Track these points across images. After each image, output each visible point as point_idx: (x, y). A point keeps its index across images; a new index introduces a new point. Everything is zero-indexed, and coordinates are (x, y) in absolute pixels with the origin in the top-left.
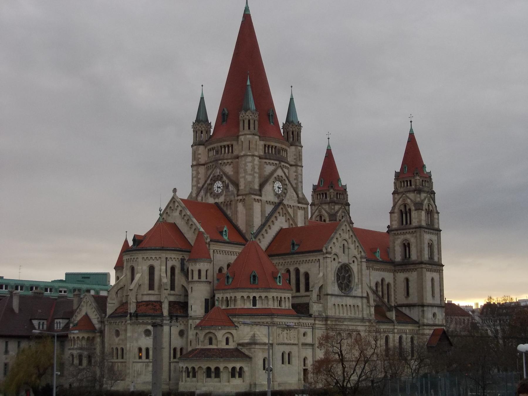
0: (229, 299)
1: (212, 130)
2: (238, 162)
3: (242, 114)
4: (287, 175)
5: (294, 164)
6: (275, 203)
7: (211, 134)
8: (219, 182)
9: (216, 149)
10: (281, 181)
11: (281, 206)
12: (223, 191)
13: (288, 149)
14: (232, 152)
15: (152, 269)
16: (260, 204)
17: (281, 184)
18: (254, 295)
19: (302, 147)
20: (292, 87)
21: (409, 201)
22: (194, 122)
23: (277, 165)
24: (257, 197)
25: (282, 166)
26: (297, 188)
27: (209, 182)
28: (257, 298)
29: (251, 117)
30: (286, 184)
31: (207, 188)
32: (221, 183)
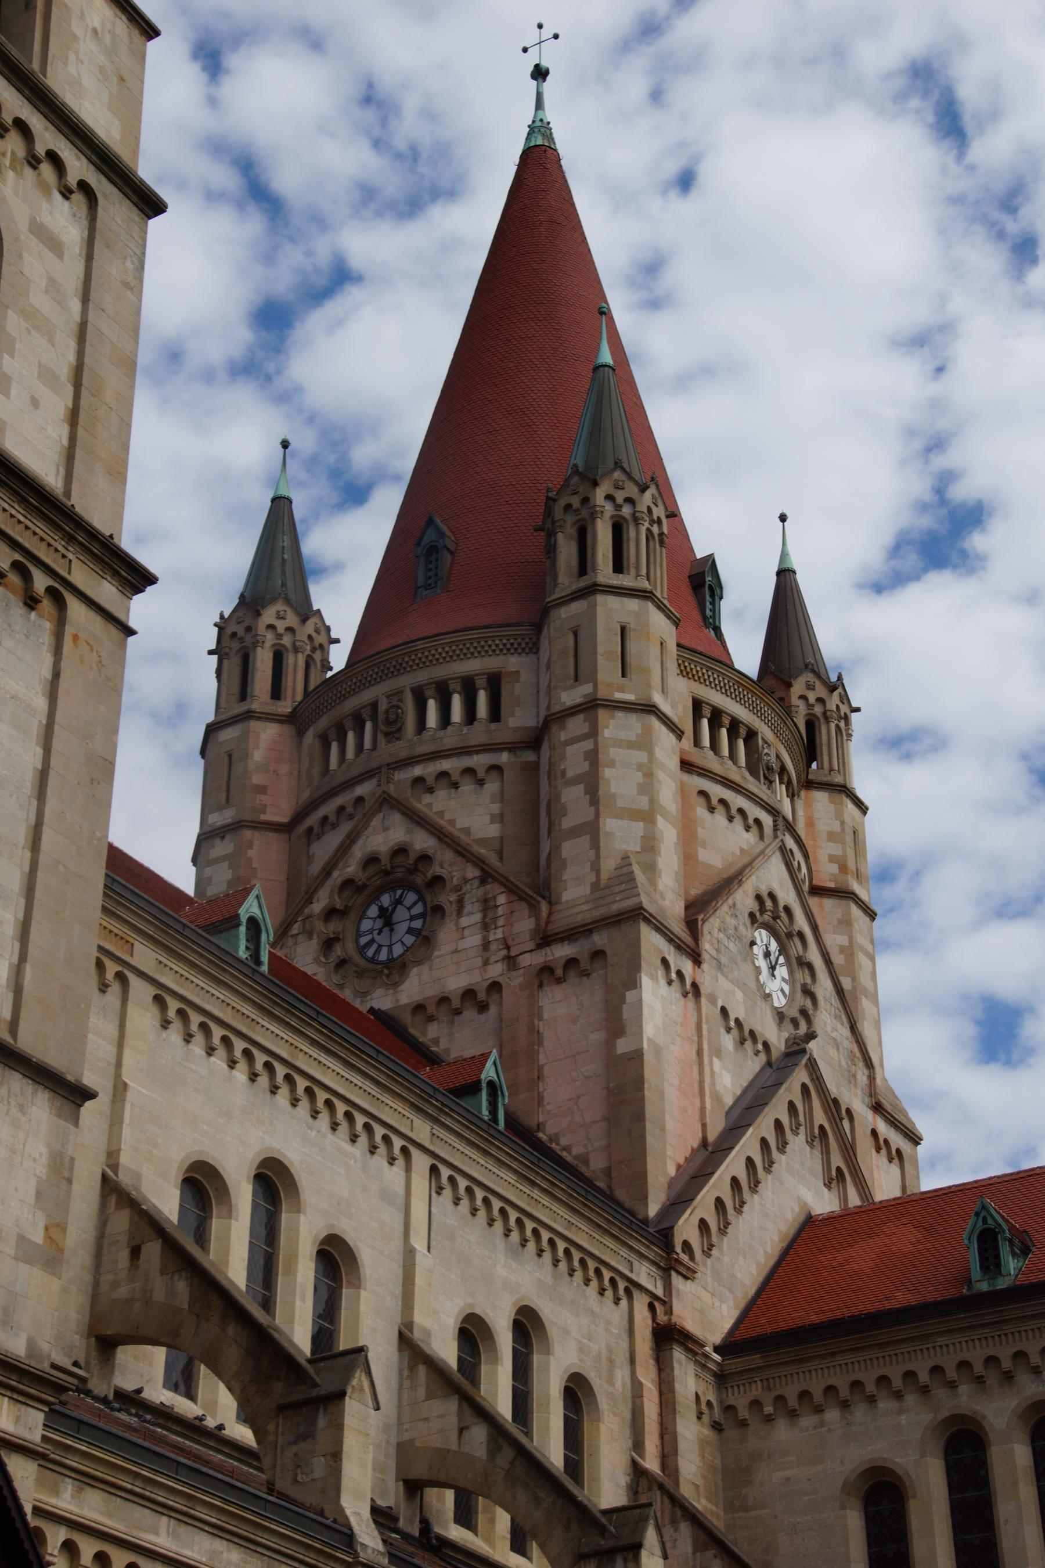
5: (832, 885)
6: (766, 1045)
9: (383, 706)
10: (786, 938)
11: (801, 1076)
14: (495, 715)
19: (862, 808)
20: (783, 518)
22: (226, 616)
29: (626, 511)
30: (810, 967)
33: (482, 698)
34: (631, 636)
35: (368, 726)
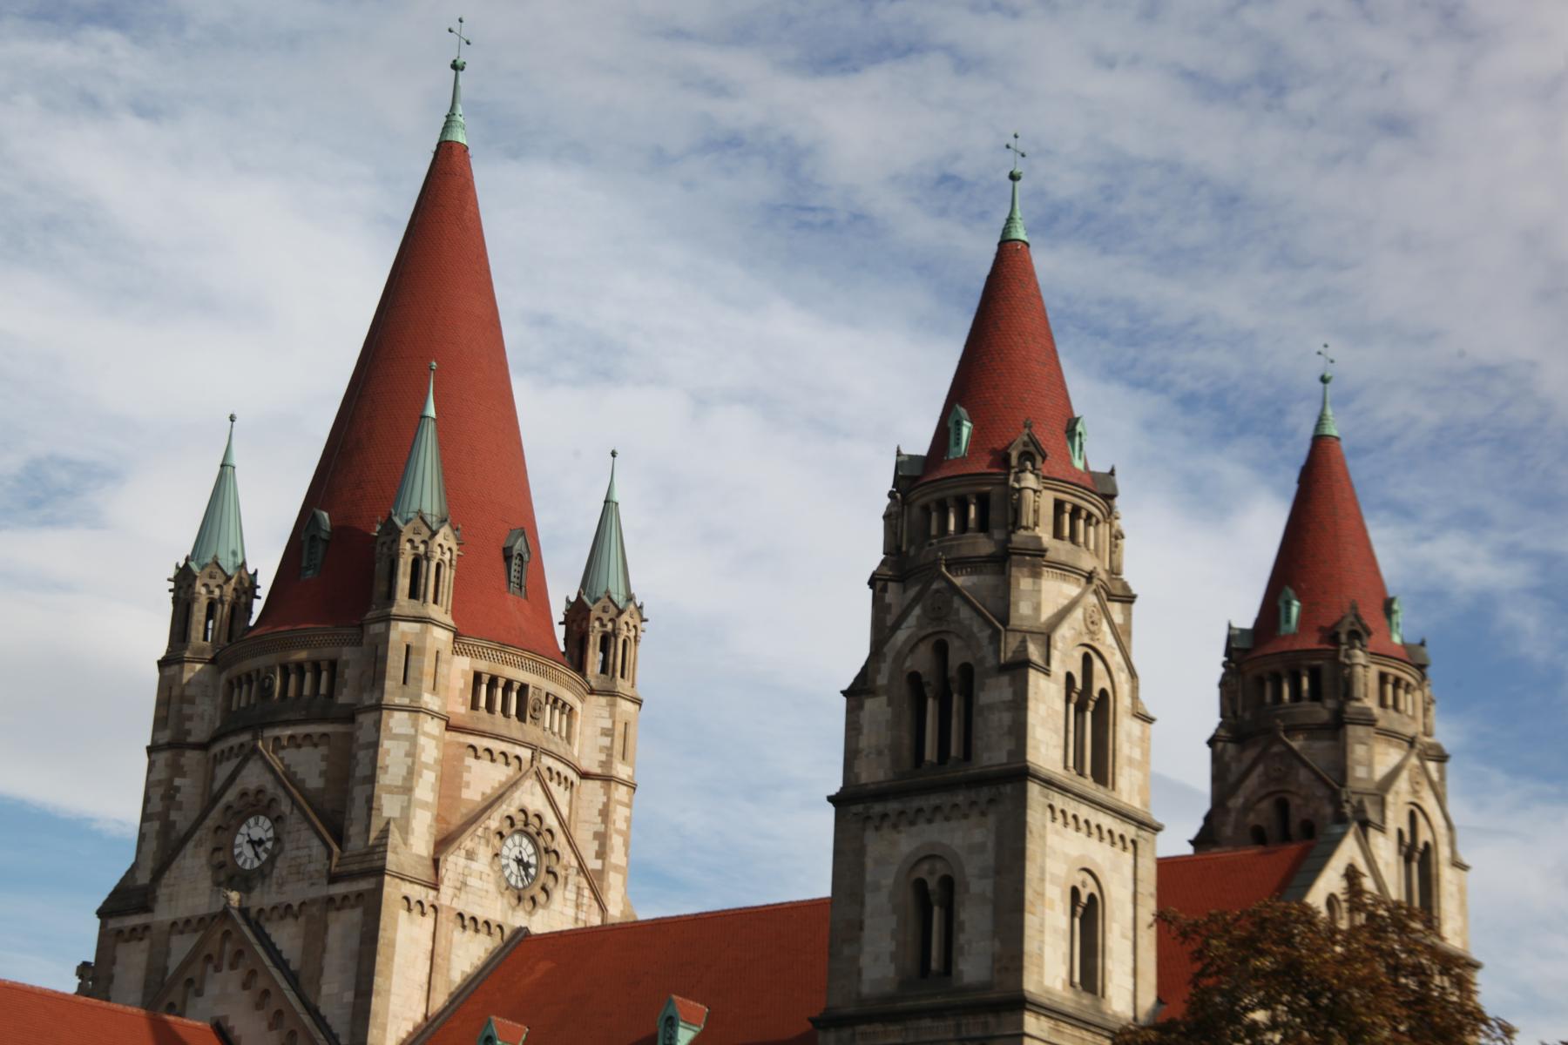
1: (258, 606)
2: (350, 737)
4: (565, 811)
5: (598, 770)
7: (252, 622)
8: (262, 818)
13: (578, 706)
16: (429, 921)
17: (530, 849)
23: (526, 765)
24: (416, 892)
25: (546, 774)
26: (601, 874)
32: (268, 824)
33: (324, 675)
34: (412, 651)
35: (255, 684)
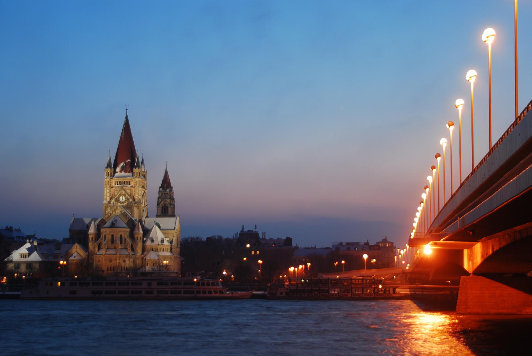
0: (154, 248)
3: (137, 169)
12: (126, 200)
15: (121, 236)
18: (164, 247)
21: (167, 202)
27: (117, 196)
28: (164, 249)
31: (117, 199)
